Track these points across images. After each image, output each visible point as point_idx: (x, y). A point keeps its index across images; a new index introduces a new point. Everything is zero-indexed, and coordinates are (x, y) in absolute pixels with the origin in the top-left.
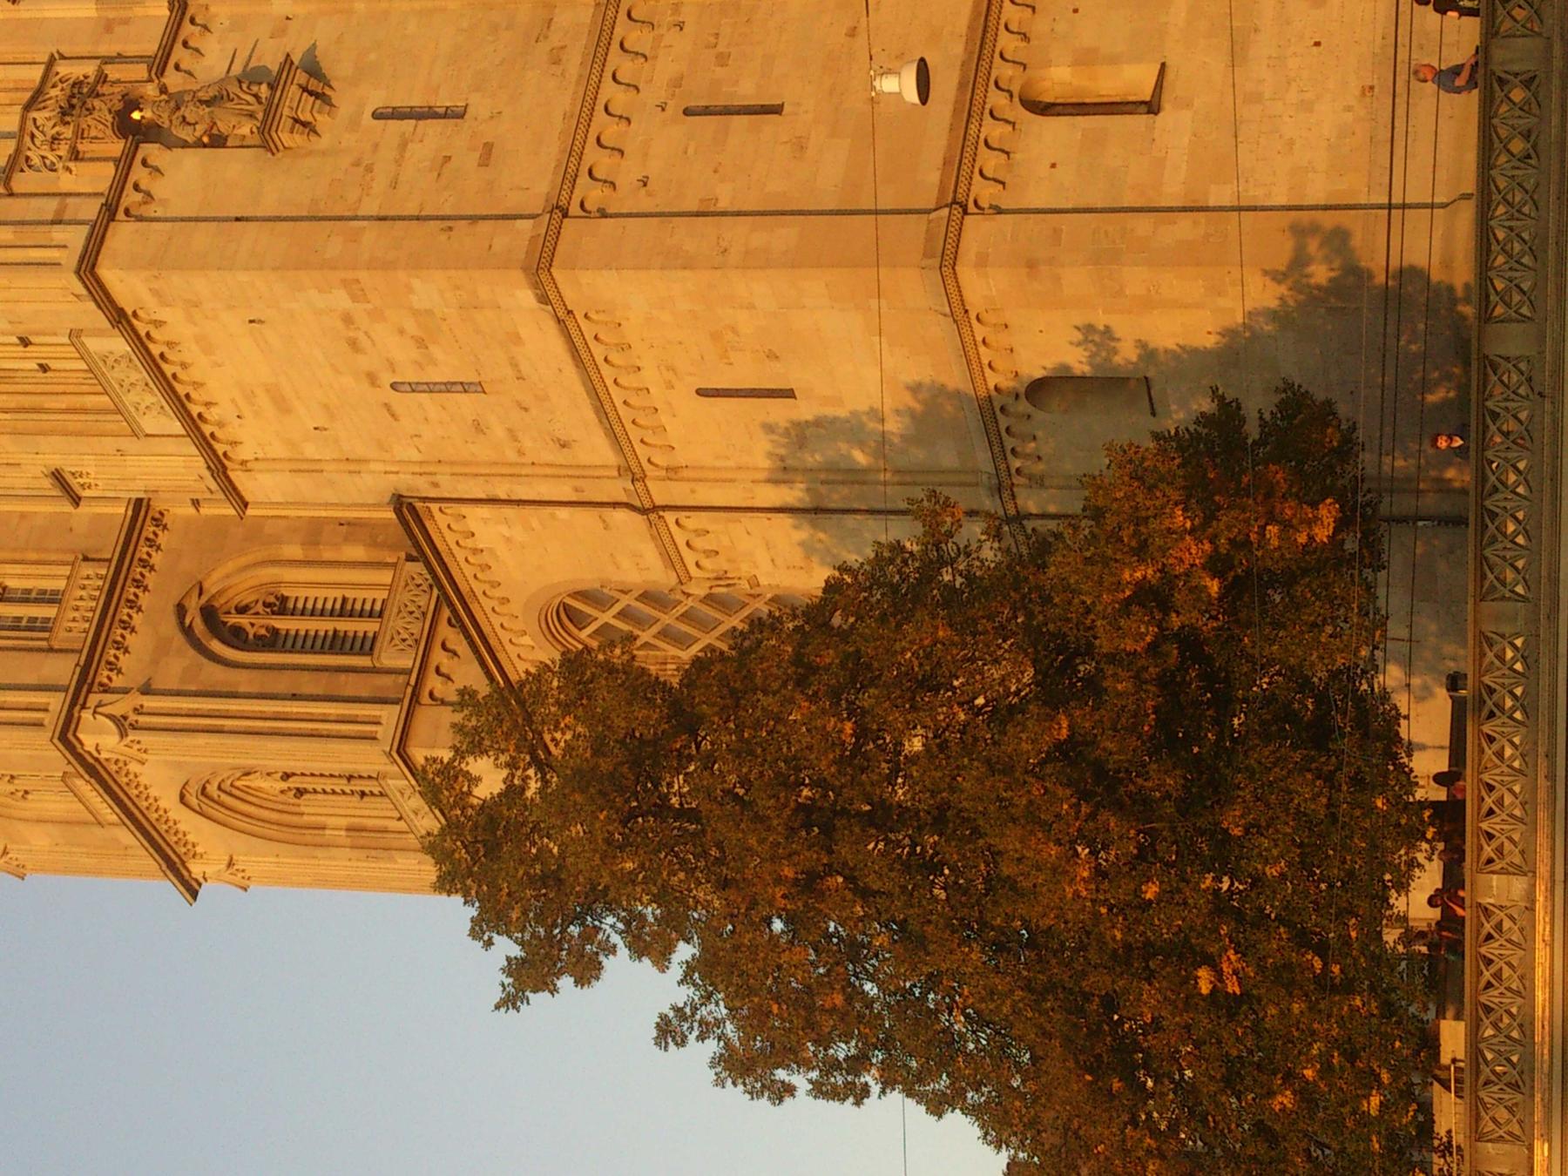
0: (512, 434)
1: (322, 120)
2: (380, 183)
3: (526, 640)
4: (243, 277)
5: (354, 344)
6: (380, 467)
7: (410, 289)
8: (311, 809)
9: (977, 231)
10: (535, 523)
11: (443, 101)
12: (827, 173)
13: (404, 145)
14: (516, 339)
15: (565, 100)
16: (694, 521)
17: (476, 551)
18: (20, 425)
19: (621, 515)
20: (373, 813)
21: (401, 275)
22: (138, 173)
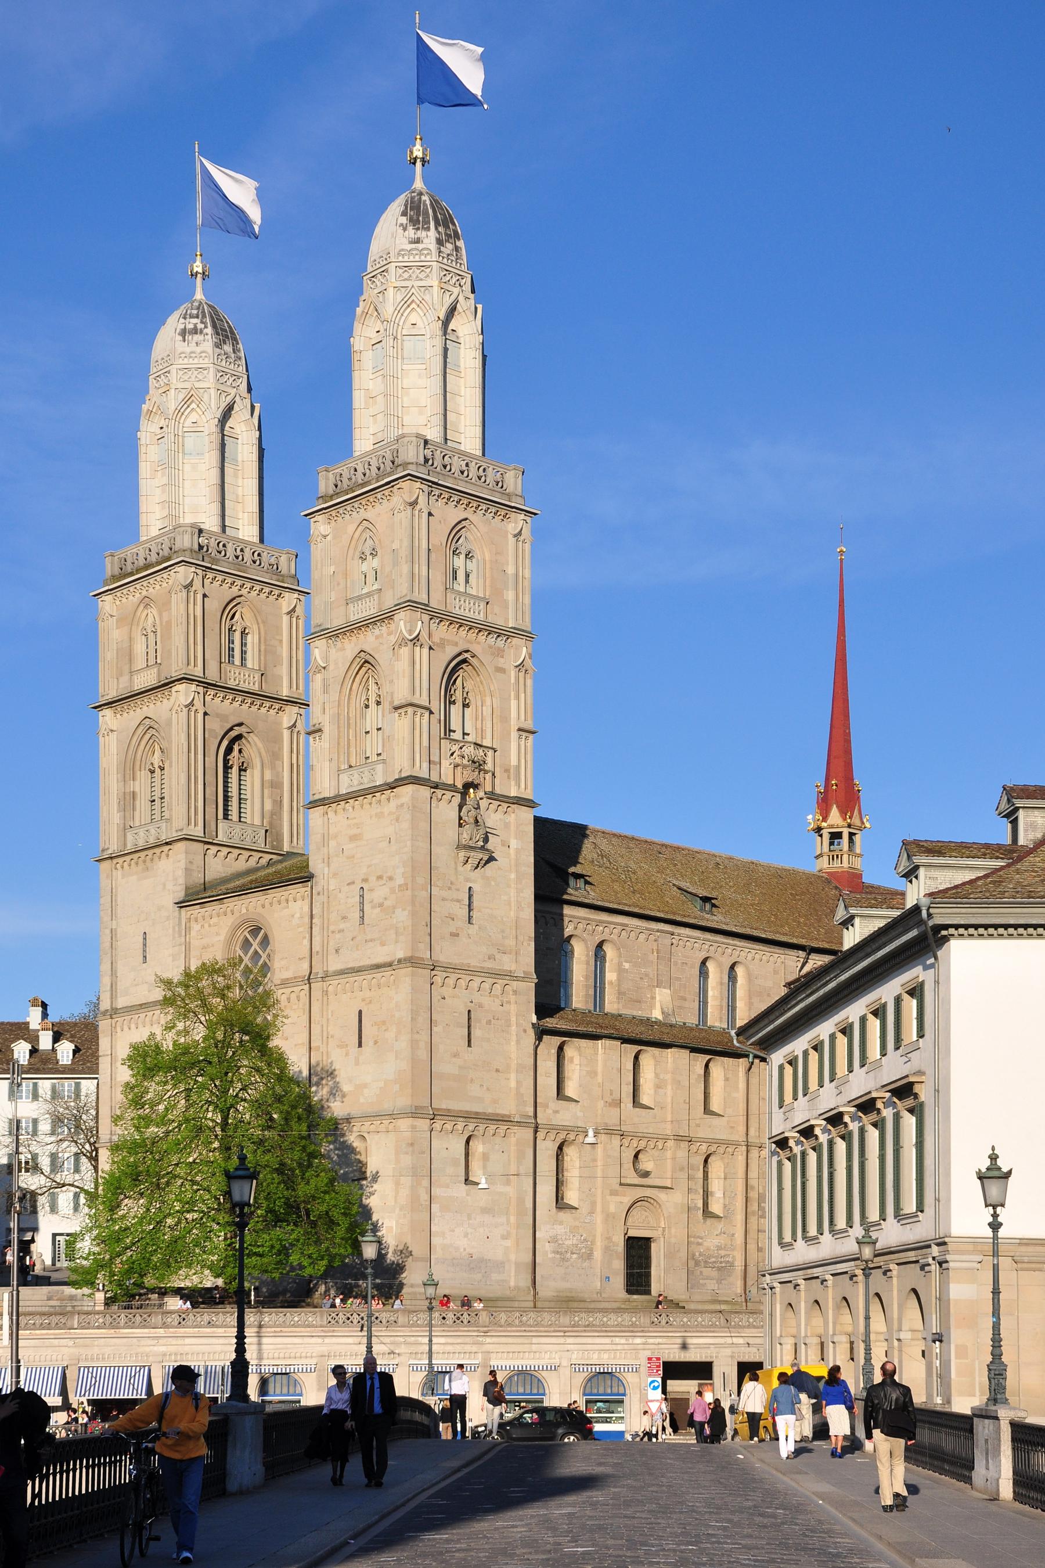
0: (341, 931)
1: (469, 866)
2: (445, 894)
3: (244, 911)
4: (409, 843)
5: (380, 877)
6: (326, 872)
7: (404, 910)
8: (143, 775)
9: (424, 1124)
10: (301, 929)
11: (474, 914)
12: (445, 1066)
13: (458, 901)
14: (383, 944)
15: (474, 963)
16: (305, 999)
17: (287, 901)
18: (342, 717)
19: (306, 965)
20: (142, 804)
21: (409, 908)
22: (449, 794)
